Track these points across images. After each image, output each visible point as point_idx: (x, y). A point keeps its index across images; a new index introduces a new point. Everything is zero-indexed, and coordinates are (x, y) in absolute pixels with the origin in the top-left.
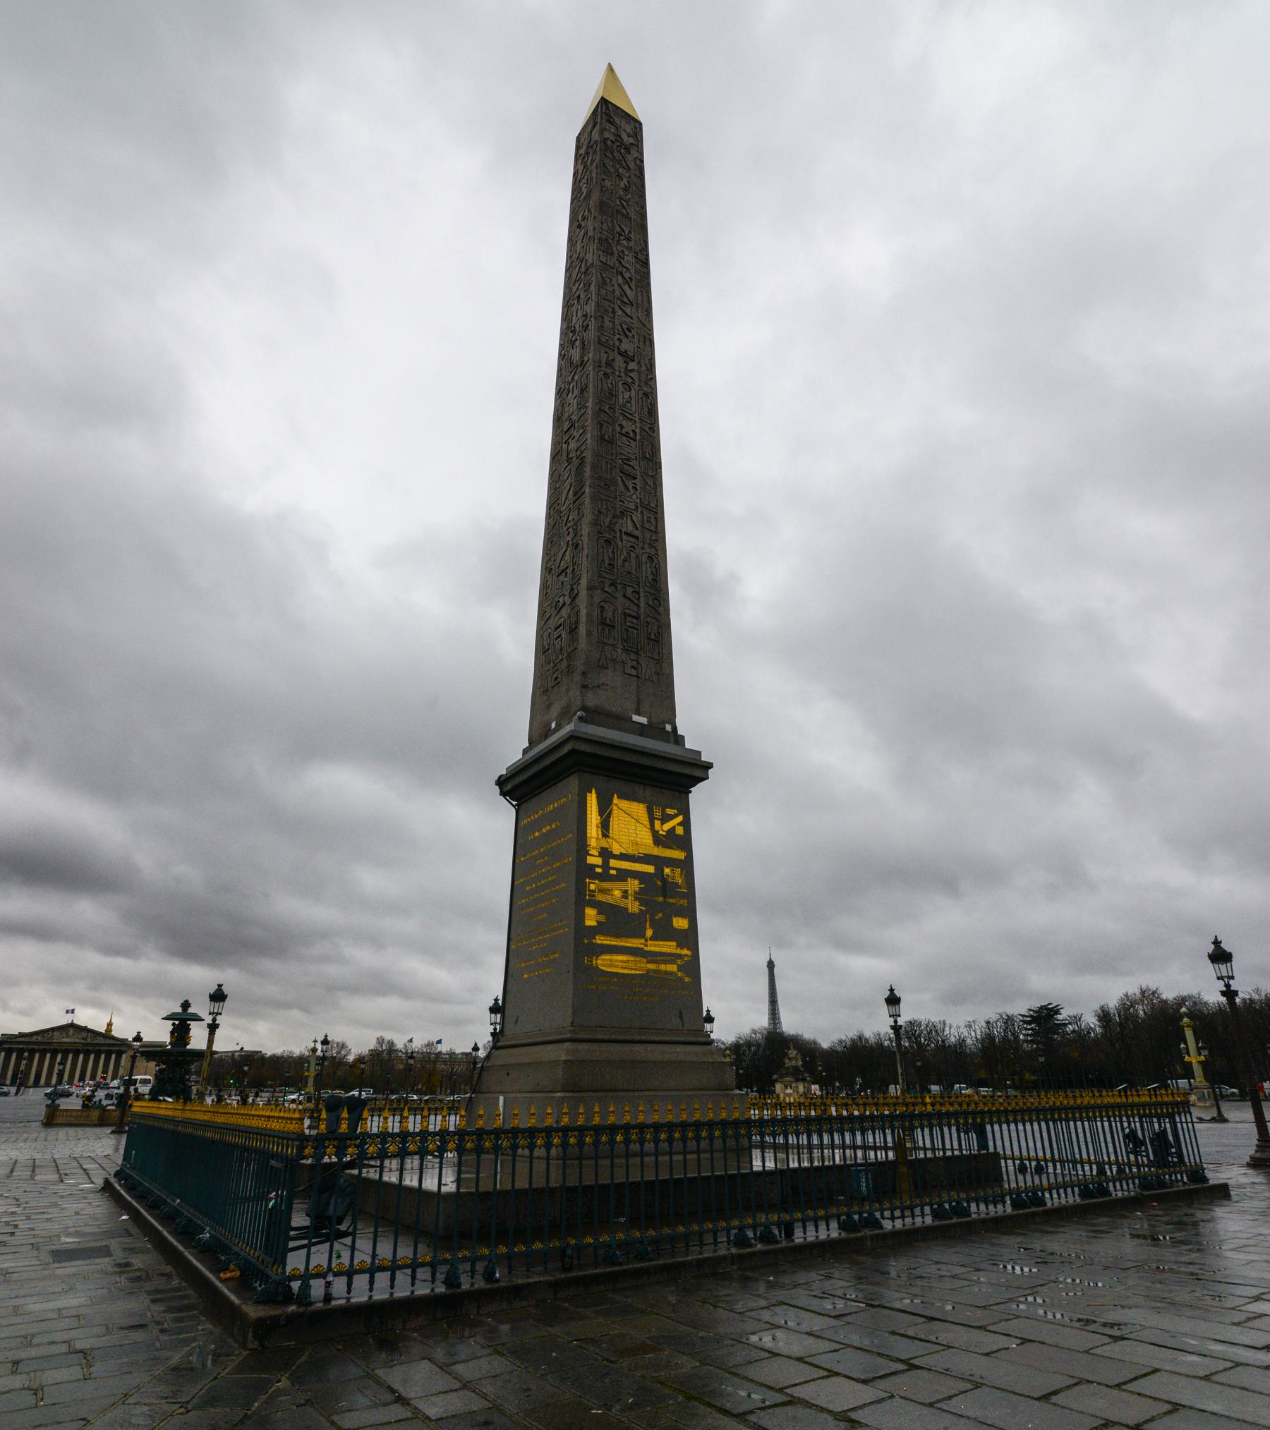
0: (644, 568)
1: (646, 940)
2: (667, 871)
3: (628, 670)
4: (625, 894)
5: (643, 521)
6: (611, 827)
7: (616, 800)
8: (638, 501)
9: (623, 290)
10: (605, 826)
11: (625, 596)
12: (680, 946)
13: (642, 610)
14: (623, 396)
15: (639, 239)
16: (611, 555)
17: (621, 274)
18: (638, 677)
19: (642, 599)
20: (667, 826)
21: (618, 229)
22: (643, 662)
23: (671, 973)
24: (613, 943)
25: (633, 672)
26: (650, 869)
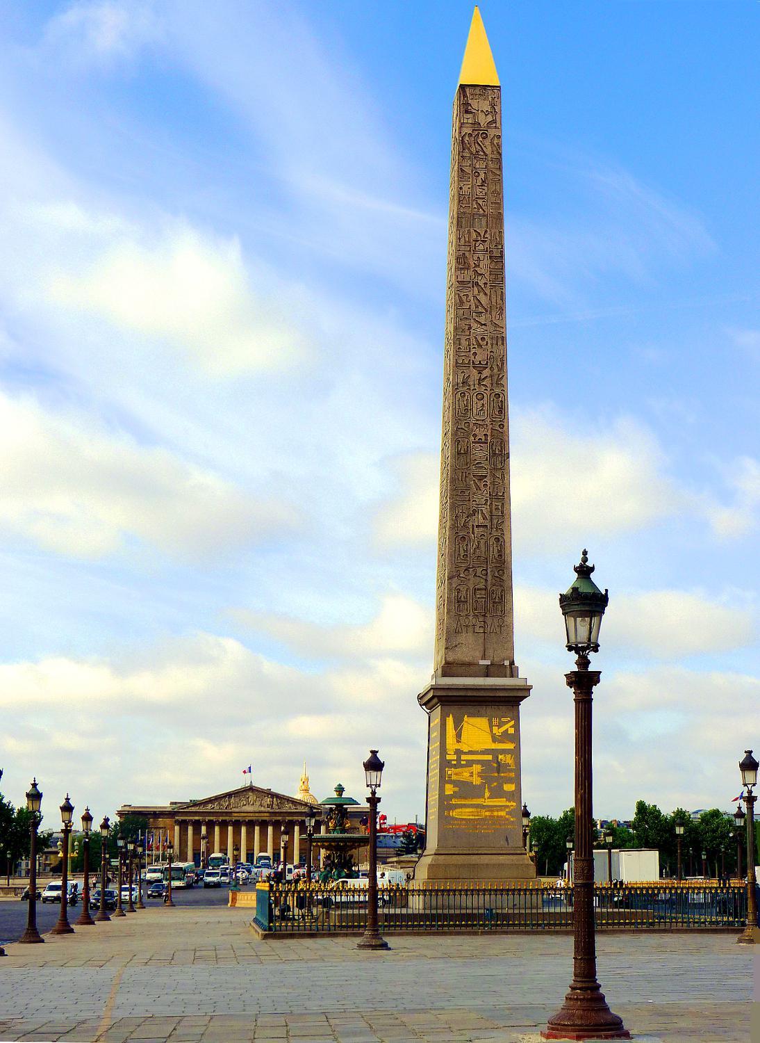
0: (491, 549)
5: (491, 512)
8: (488, 495)
10: (459, 736)
13: (489, 582)
14: (476, 405)
15: (495, 233)
17: (477, 284)
21: (474, 235)
22: (489, 621)
23: (501, 817)
24: (464, 803)
26: (489, 757)
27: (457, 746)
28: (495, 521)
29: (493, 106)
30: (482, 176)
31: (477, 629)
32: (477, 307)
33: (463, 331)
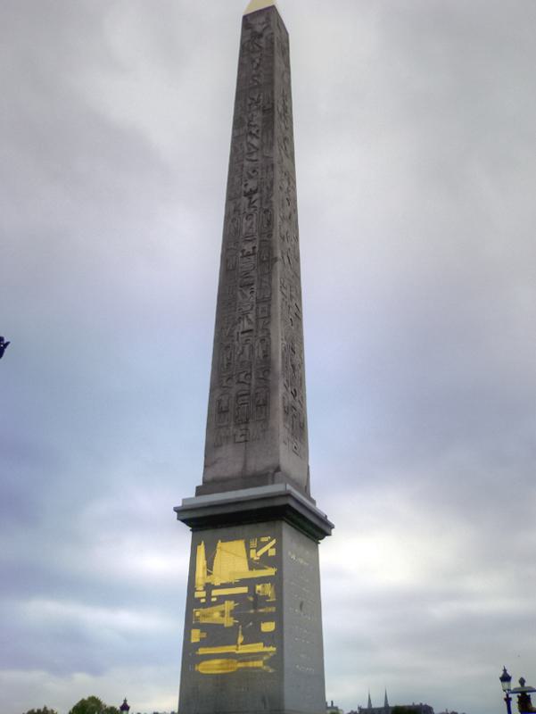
0: (256, 352)
1: (238, 646)
2: (259, 587)
3: (238, 439)
6: (214, 567)
7: (220, 544)
8: (254, 300)
10: (210, 566)
11: (239, 382)
12: (266, 645)
13: (253, 386)
14: (245, 224)
16: (229, 357)
17: (251, 133)
19: (253, 377)
20: (261, 552)
21: (249, 101)
22: (249, 428)
23: (257, 668)
25: (243, 439)
26: (244, 590)
27: (208, 580)
28: (261, 325)
30: (257, 61)
31: (239, 439)
32: (249, 149)
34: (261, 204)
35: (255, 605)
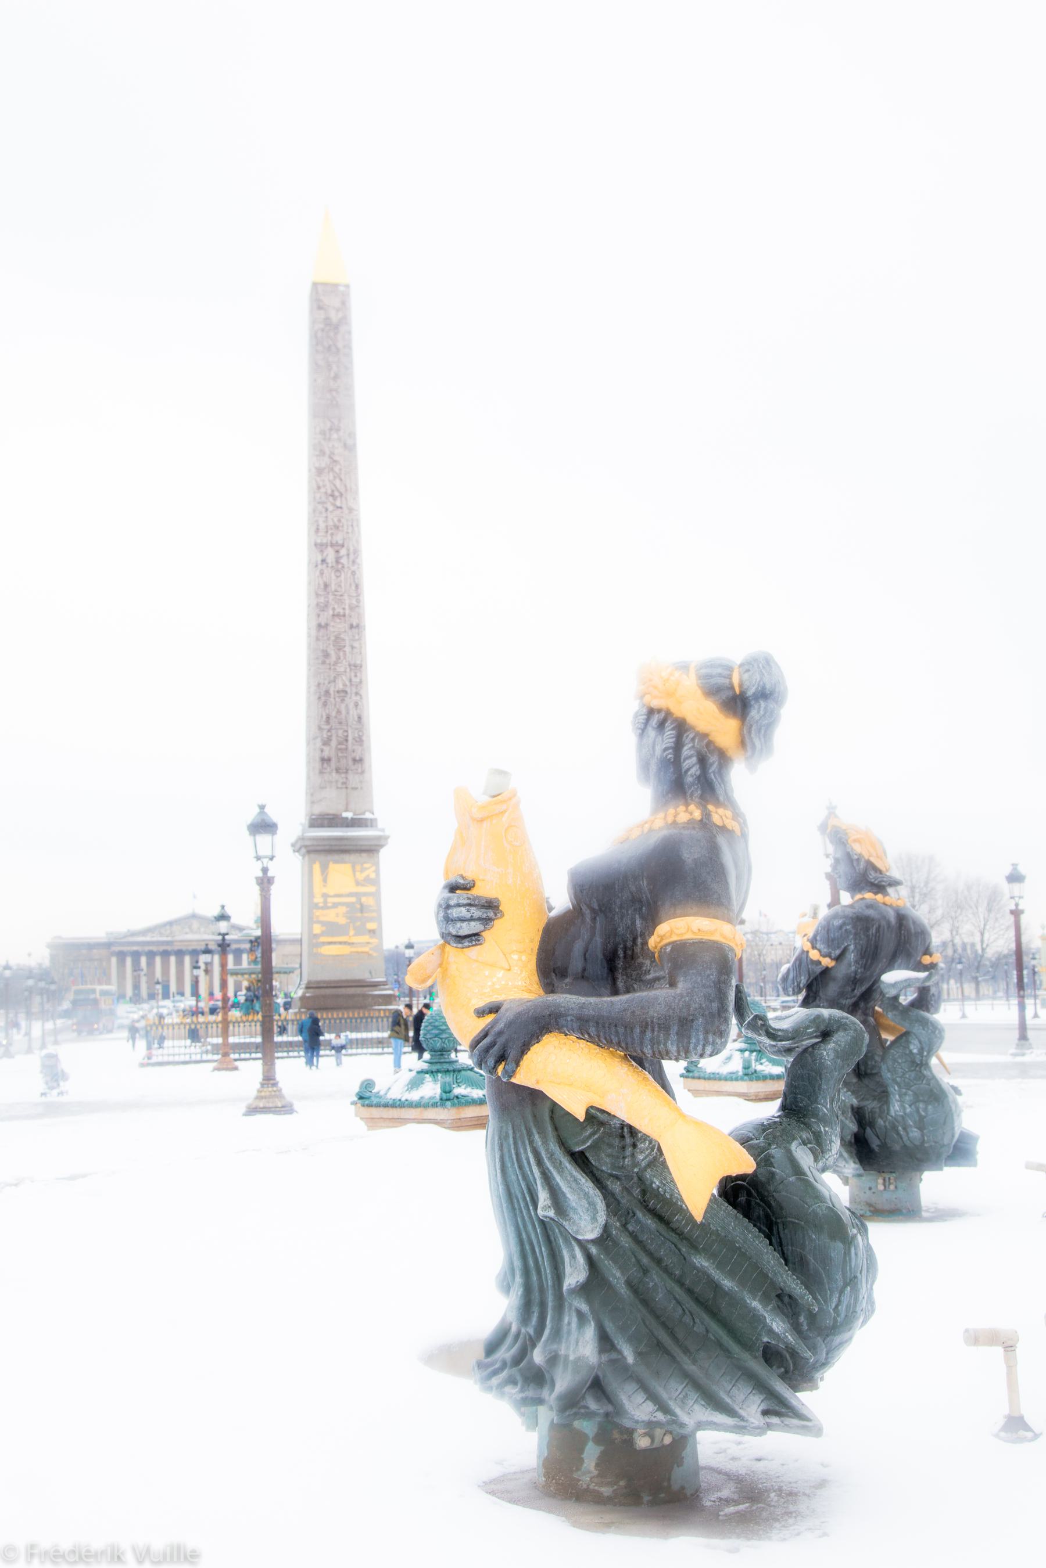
1: (350, 937)
4: (337, 915)
9: (335, 485)
10: (325, 880)
18: (347, 788)
20: (364, 874)
26: (353, 899)
27: (325, 890)
29: (344, 303)
32: (333, 491)
33: (321, 513)
34: (348, 562)
35: (362, 911)
